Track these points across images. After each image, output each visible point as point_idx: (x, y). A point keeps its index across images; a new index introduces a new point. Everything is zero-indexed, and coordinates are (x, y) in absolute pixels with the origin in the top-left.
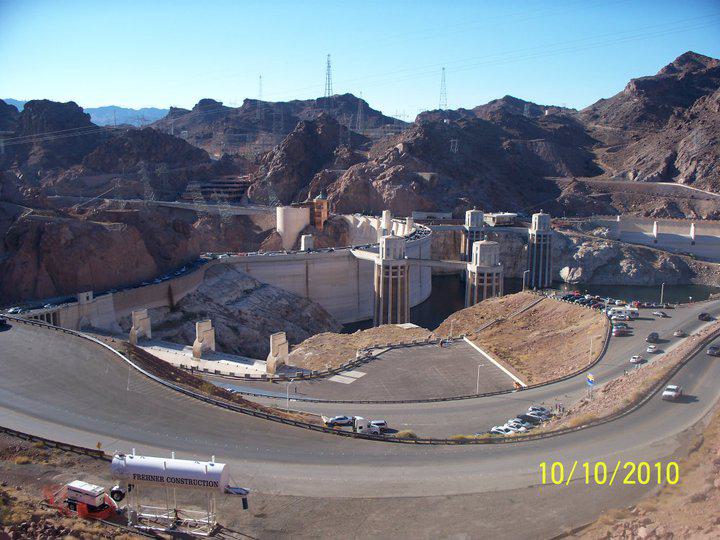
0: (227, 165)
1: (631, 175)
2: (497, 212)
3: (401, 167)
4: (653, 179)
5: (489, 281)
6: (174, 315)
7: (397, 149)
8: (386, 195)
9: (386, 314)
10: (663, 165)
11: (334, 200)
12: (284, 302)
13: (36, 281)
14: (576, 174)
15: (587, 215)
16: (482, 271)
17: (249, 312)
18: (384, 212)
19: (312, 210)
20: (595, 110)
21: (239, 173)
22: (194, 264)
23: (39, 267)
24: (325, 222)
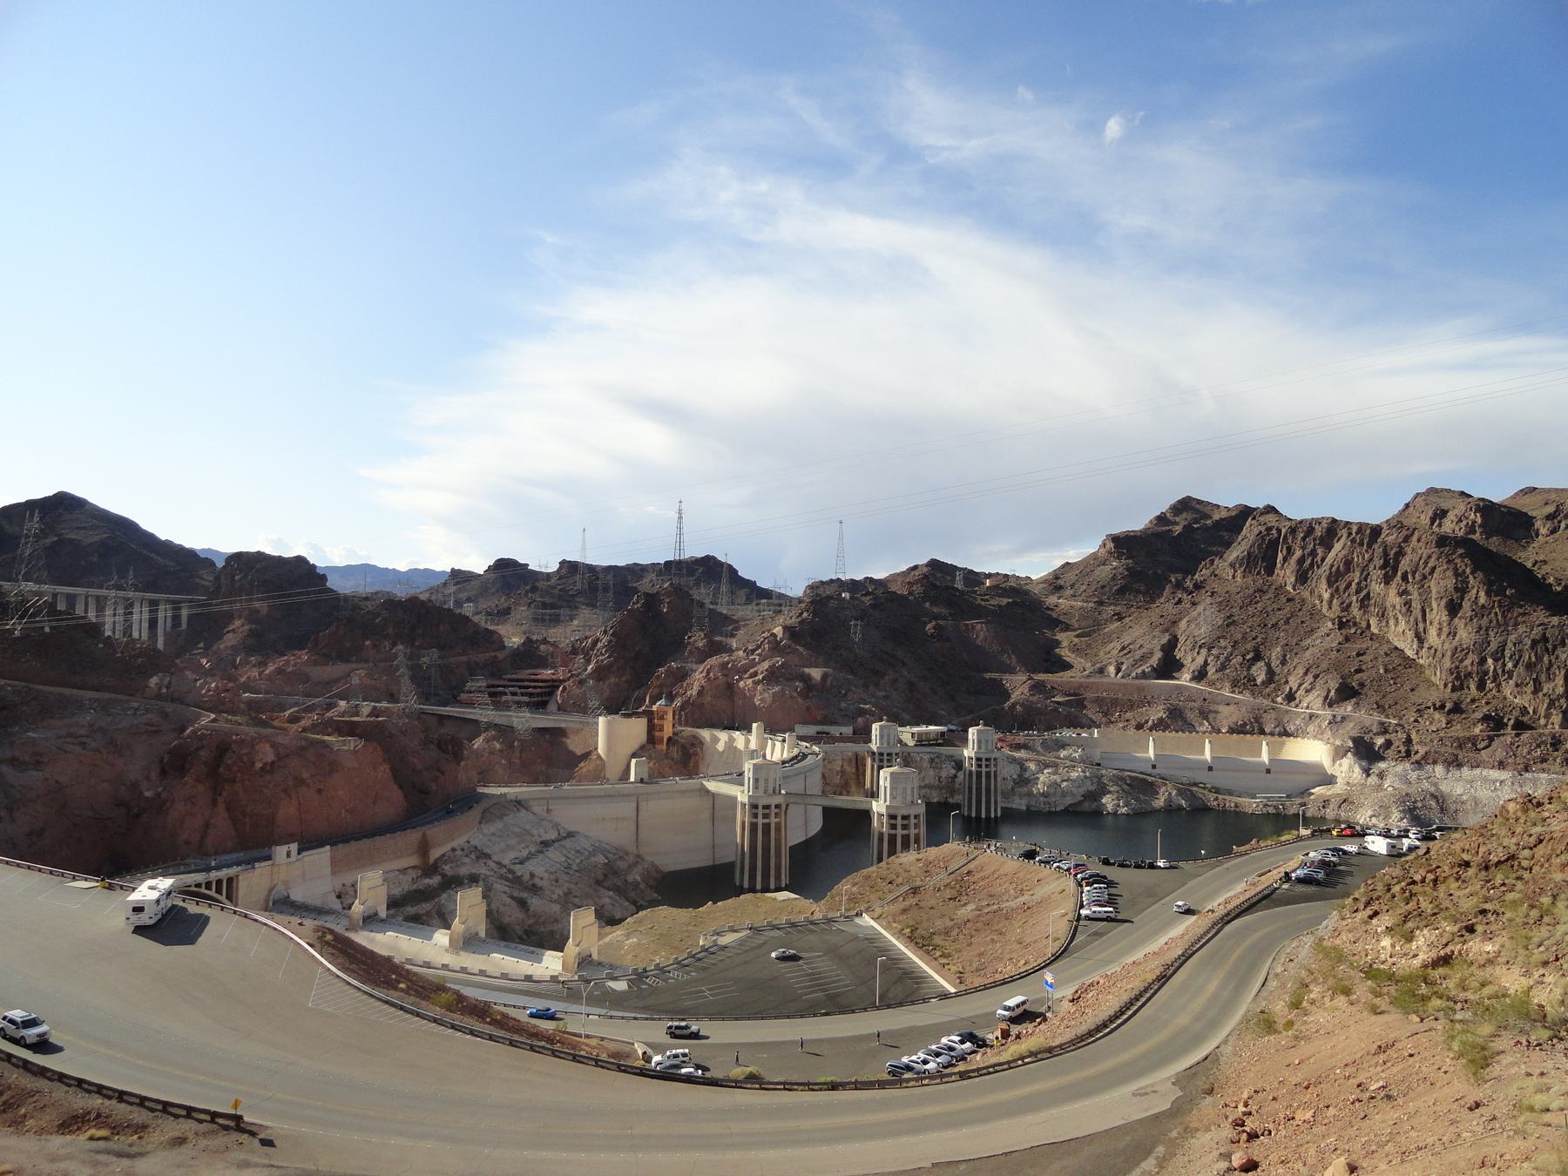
0: (529, 655)
1: (1112, 669)
2: (918, 725)
3: (779, 661)
4: (1144, 675)
6: (427, 881)
7: (774, 635)
8: (762, 696)
10: (1158, 655)
11: (682, 707)
12: (601, 859)
13: (207, 825)
15: (1050, 728)
16: (893, 812)
18: (755, 725)
19: (650, 721)
20: (1057, 578)
21: (546, 667)
22: (467, 800)
23: (214, 802)
24: (669, 739)
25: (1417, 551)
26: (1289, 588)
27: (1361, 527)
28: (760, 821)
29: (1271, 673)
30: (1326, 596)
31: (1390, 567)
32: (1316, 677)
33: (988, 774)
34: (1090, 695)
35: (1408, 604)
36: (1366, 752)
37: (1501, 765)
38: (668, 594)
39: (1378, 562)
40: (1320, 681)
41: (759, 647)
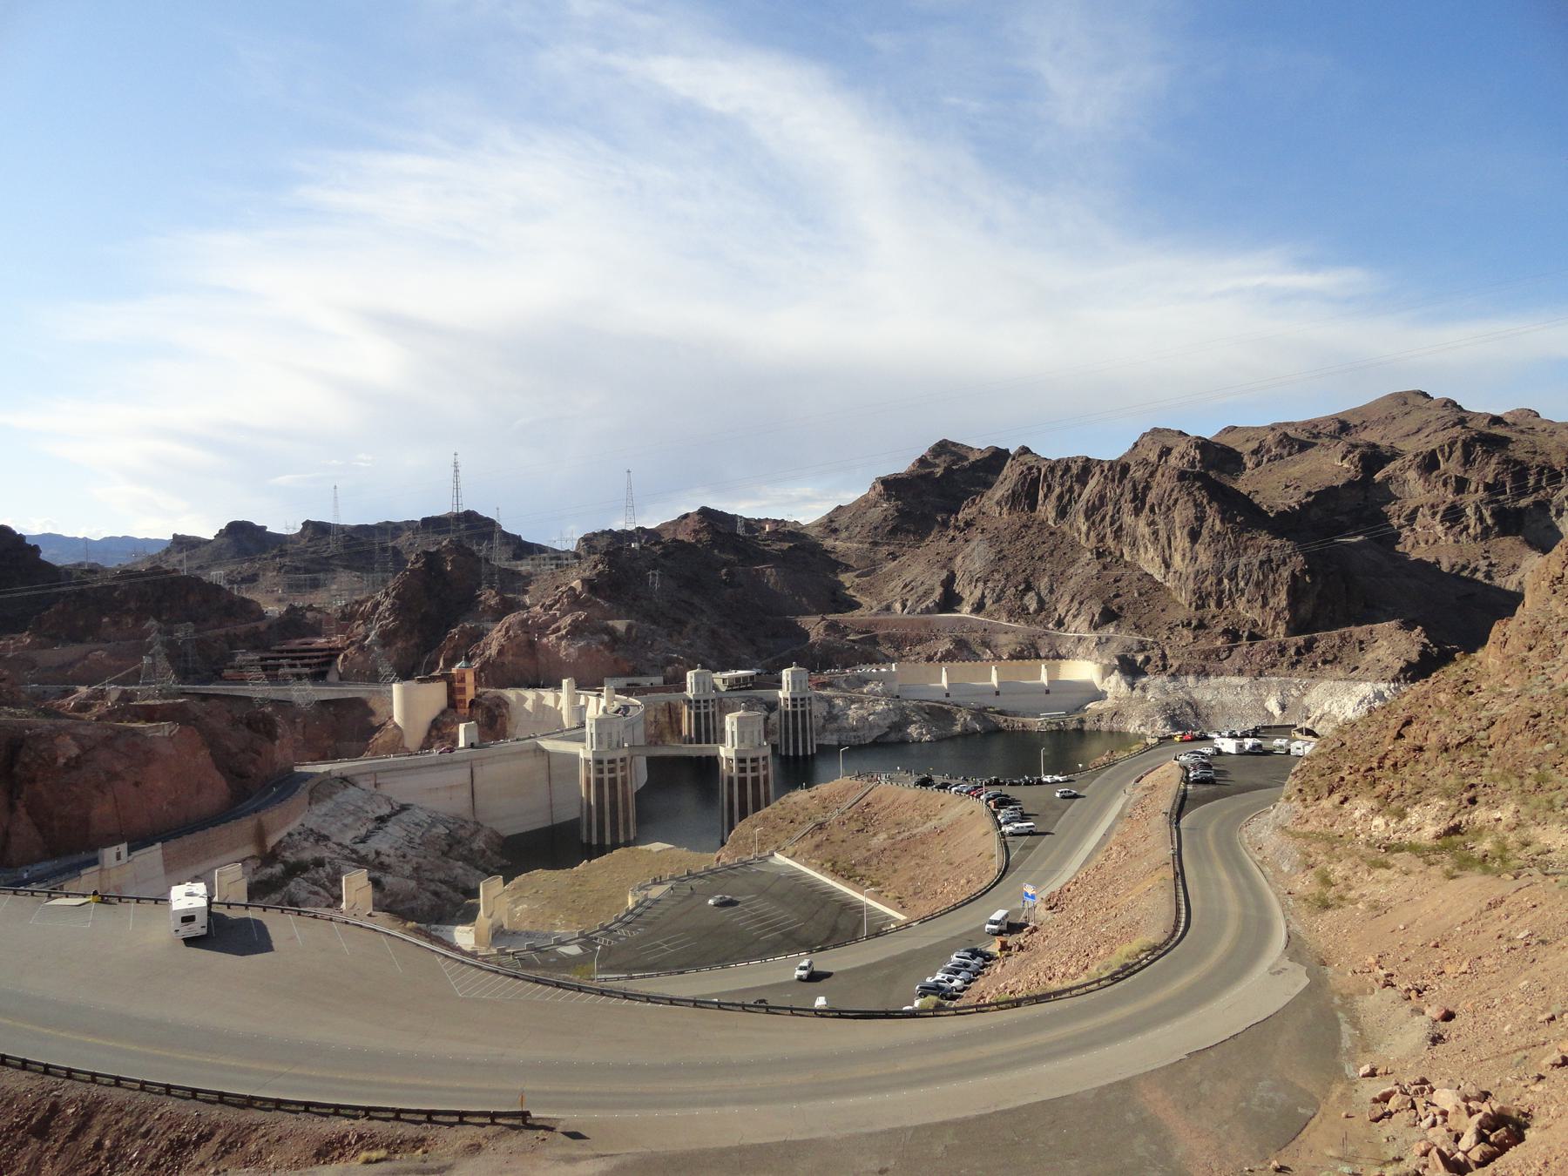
0: (294, 623)
1: (898, 606)
3: (582, 615)
4: (928, 610)
5: (753, 769)
6: (269, 871)
7: (572, 589)
8: (568, 651)
9: (615, 832)
10: (939, 590)
11: (481, 669)
12: (441, 830)
14: (823, 610)
16: (742, 756)
17: (392, 852)
18: (565, 682)
21: (319, 635)
22: (286, 784)
23: (12, 807)
24: (472, 702)
25: (1163, 484)
26: (1051, 523)
27: (1112, 464)
28: (606, 776)
29: (1041, 602)
30: (1084, 528)
31: (1139, 501)
32: (1081, 603)
33: (803, 713)
34: (881, 632)
35: (1155, 533)
36: (1130, 669)
37: (1241, 672)
38: (450, 551)
39: (1128, 496)
40: (1085, 607)
41: (557, 602)
